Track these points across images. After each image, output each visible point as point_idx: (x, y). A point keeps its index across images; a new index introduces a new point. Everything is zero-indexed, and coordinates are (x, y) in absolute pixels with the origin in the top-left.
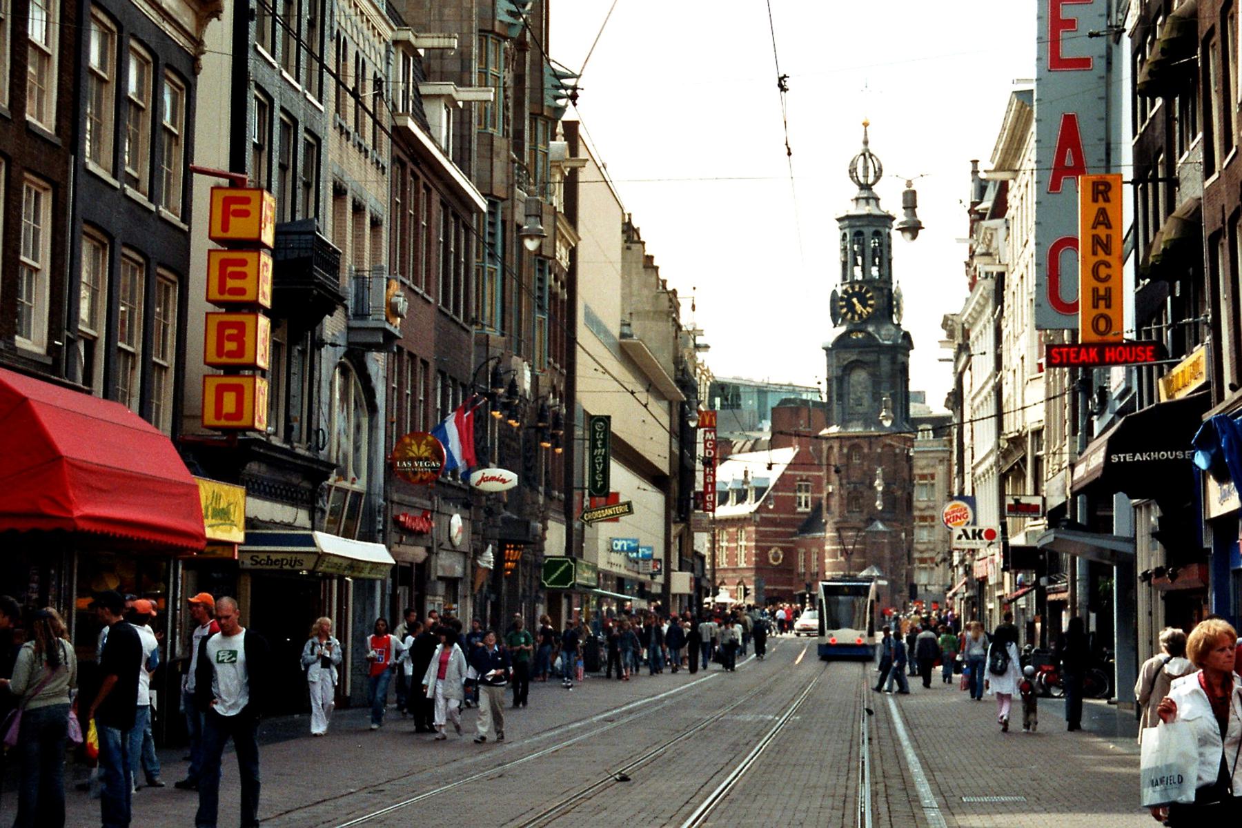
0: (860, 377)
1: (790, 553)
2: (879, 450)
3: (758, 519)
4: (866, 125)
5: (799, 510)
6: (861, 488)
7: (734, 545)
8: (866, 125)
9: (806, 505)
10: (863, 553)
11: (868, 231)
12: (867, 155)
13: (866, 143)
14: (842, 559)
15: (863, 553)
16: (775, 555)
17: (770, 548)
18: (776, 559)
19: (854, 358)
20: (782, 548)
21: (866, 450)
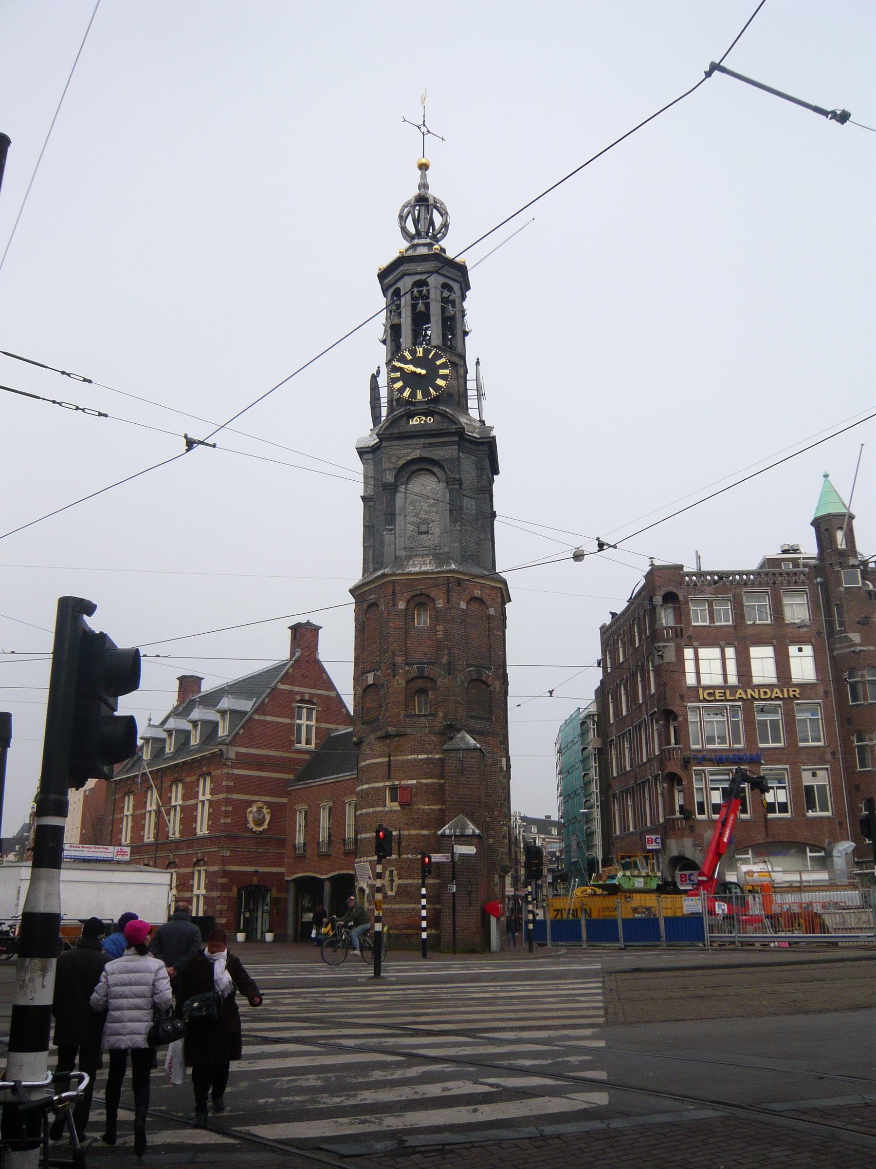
0: (426, 487)
1: (281, 816)
2: (463, 605)
3: (232, 755)
4: (423, 167)
5: (298, 746)
6: (428, 671)
7: (191, 802)
8: (423, 167)
9: (308, 742)
10: (438, 793)
11: (435, 281)
12: (423, 201)
13: (424, 186)
14: (396, 806)
15: (438, 793)
16: (257, 814)
17: (250, 803)
18: (259, 823)
19: (417, 454)
20: (269, 805)
21: (440, 604)
